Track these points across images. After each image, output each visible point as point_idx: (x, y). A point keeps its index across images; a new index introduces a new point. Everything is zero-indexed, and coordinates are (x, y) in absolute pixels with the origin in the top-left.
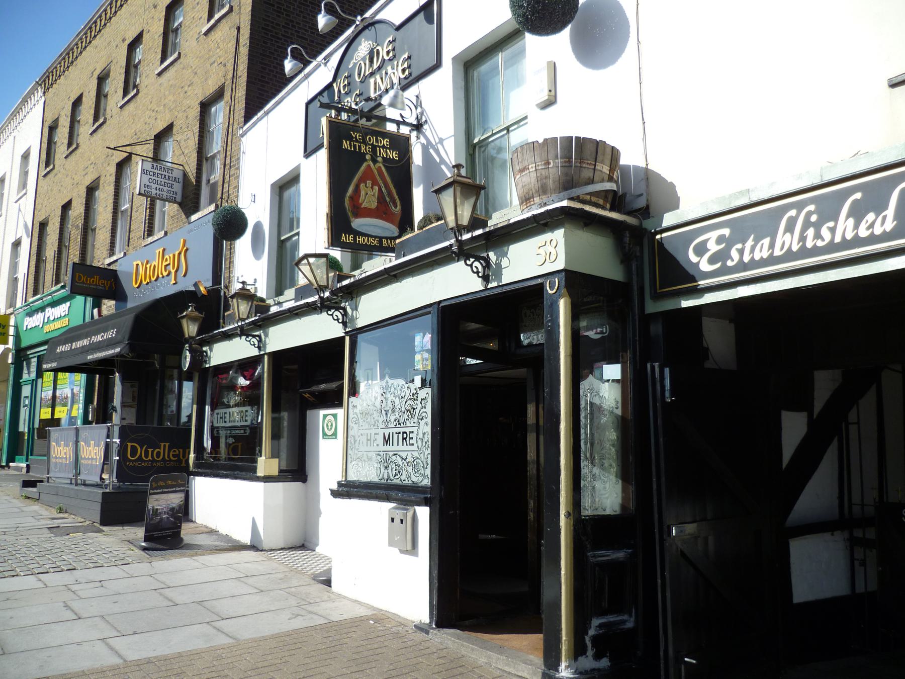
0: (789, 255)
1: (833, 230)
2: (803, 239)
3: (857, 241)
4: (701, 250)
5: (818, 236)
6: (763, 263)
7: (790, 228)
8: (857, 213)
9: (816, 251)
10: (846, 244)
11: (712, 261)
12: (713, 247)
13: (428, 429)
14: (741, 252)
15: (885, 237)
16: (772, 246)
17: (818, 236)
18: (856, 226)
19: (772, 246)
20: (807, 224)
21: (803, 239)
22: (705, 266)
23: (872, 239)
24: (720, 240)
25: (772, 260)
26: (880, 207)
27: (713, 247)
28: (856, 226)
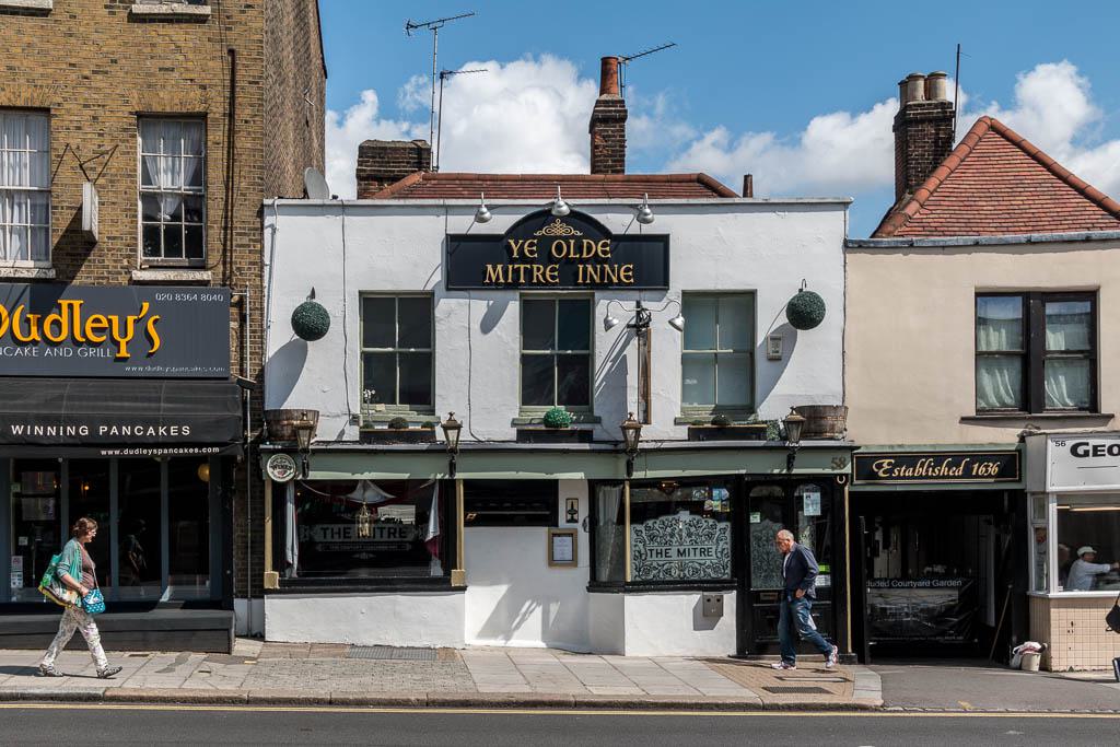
0: (921, 477)
1: (940, 471)
2: (927, 471)
3: (948, 477)
4: (880, 466)
5: (933, 471)
6: (909, 478)
7: (922, 465)
8: (949, 466)
9: (932, 477)
10: (944, 477)
11: (884, 472)
12: (886, 466)
13: (728, 546)
14: (899, 471)
15: (958, 477)
16: (914, 471)
17: (933, 471)
18: (949, 471)
19: (914, 471)
20: (929, 466)
21: (927, 471)
22: (881, 474)
23: (954, 477)
24: (889, 464)
25: (913, 477)
26: (958, 466)
27: (886, 466)
28: (949, 471)
